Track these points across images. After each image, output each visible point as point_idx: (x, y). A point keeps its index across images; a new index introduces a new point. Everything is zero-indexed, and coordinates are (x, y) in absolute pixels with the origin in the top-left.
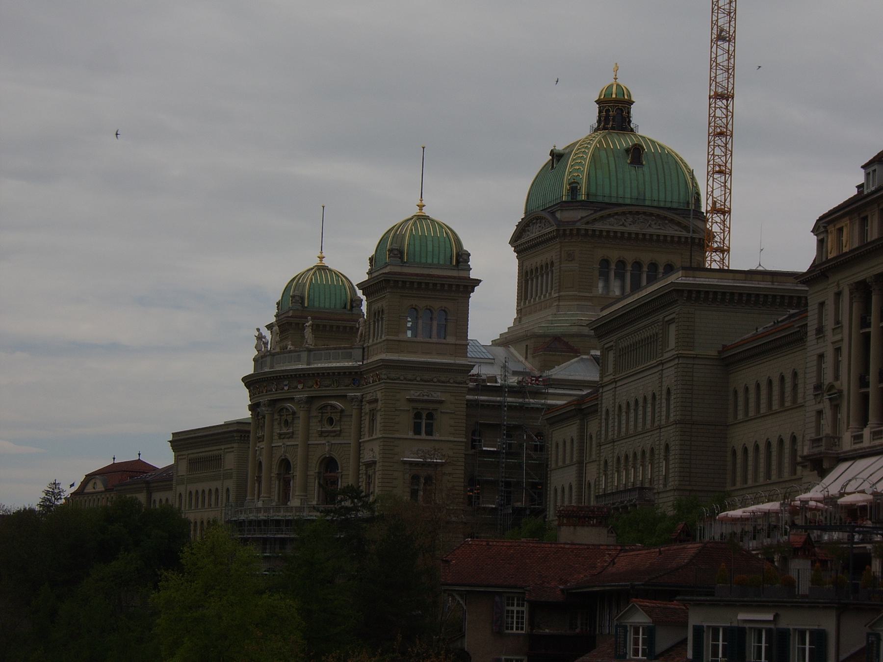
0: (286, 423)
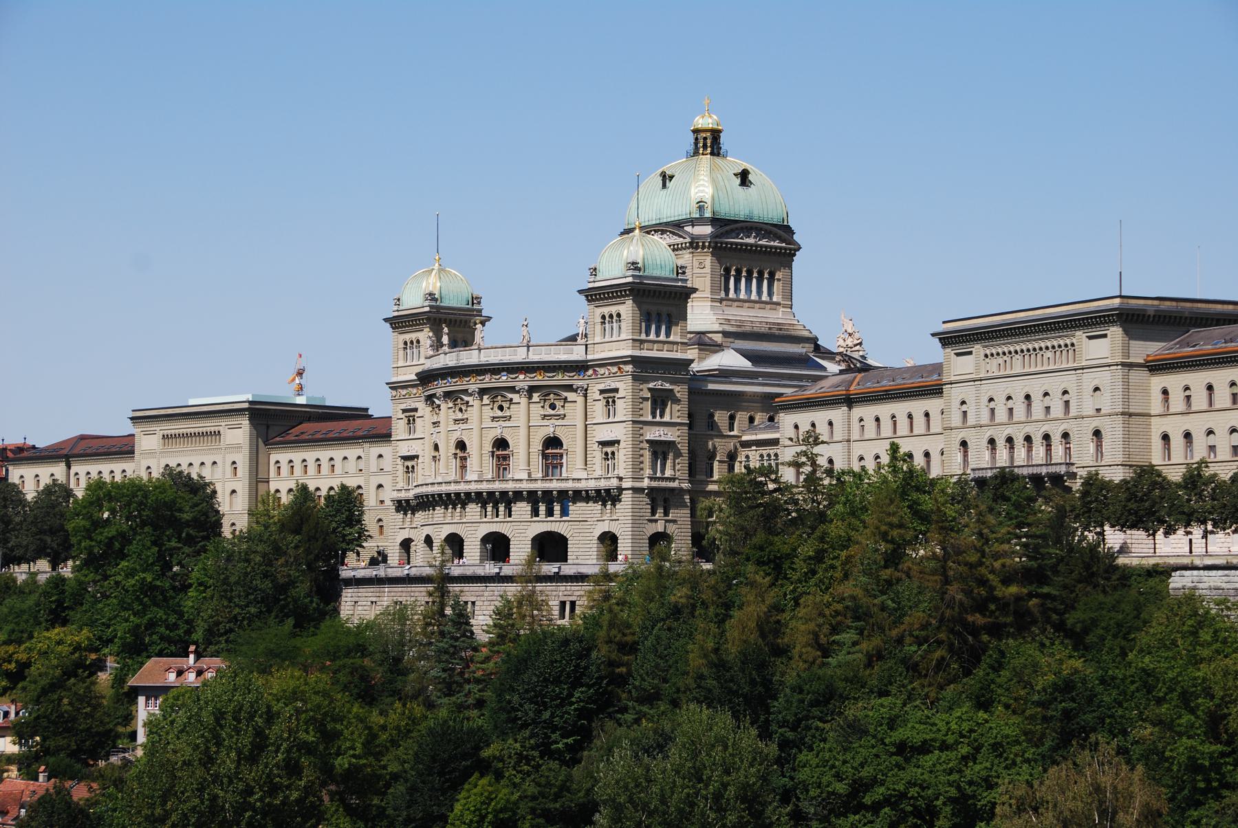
0: (461, 410)
